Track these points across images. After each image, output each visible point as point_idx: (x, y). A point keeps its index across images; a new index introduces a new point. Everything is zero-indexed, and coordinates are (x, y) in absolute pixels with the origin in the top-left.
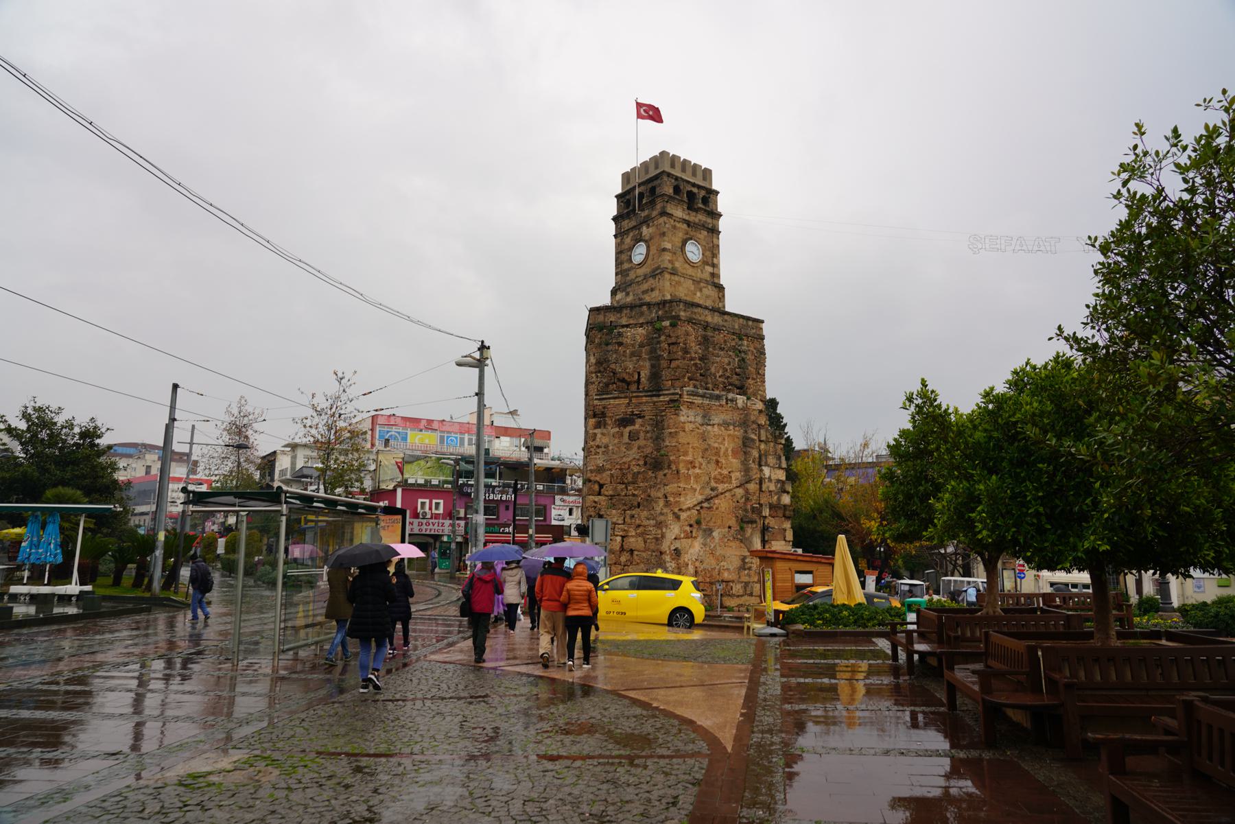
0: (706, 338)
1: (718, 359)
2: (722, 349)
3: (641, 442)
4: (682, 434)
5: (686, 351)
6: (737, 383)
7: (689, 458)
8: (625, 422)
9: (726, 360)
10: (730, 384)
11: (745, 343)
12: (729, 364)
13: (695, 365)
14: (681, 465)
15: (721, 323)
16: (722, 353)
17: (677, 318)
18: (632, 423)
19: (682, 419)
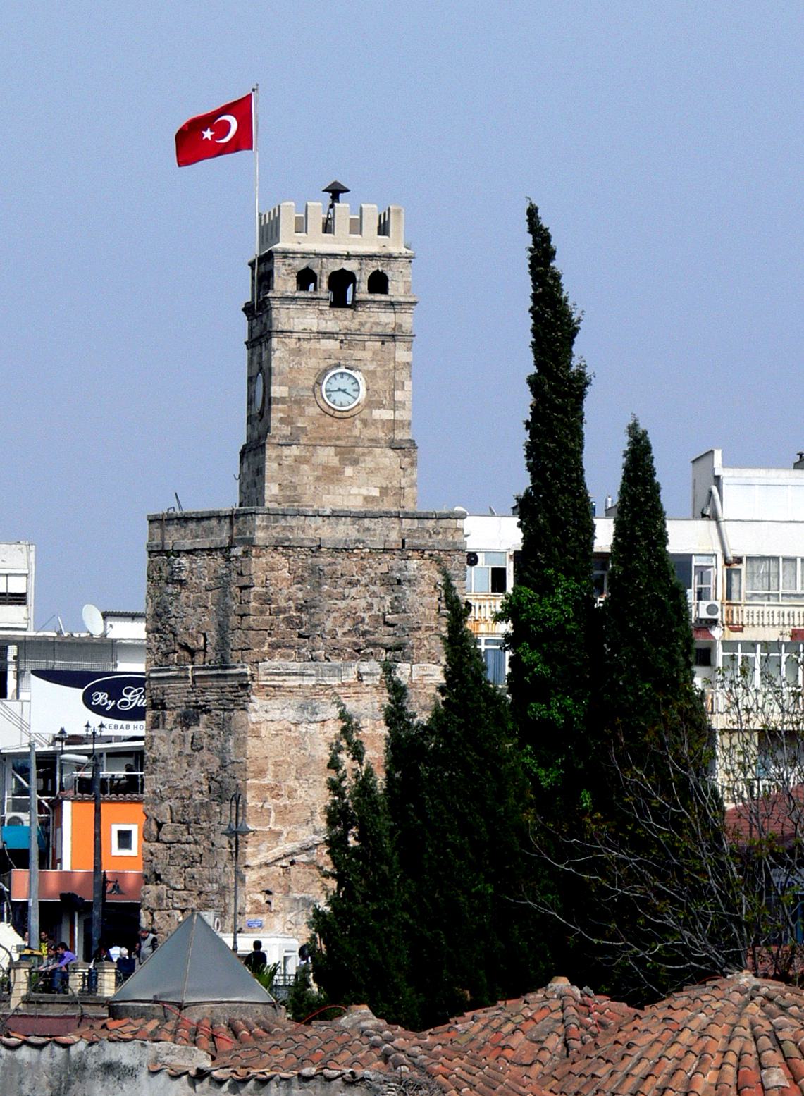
0: (315, 571)
1: (342, 604)
2: (352, 584)
3: (205, 756)
4: (252, 742)
5: (266, 599)
6: (388, 640)
7: (268, 780)
8: (187, 719)
9: (362, 604)
10: (374, 645)
11: (413, 564)
12: (370, 607)
13: (289, 620)
14: (249, 795)
15: (354, 535)
16: (354, 591)
17: (250, 543)
18: (196, 721)
19: (253, 717)
